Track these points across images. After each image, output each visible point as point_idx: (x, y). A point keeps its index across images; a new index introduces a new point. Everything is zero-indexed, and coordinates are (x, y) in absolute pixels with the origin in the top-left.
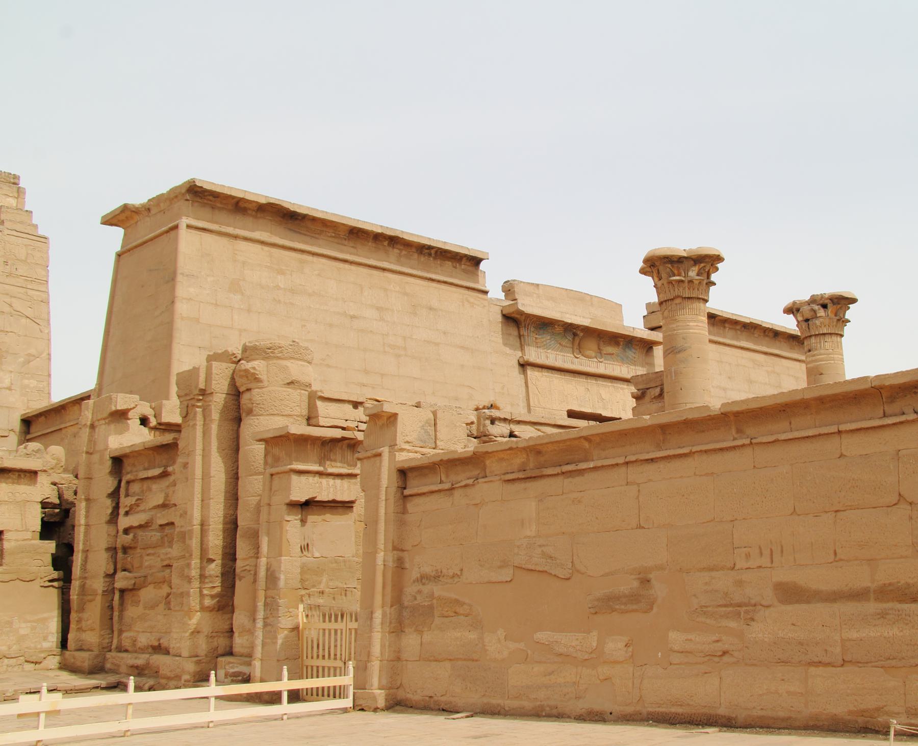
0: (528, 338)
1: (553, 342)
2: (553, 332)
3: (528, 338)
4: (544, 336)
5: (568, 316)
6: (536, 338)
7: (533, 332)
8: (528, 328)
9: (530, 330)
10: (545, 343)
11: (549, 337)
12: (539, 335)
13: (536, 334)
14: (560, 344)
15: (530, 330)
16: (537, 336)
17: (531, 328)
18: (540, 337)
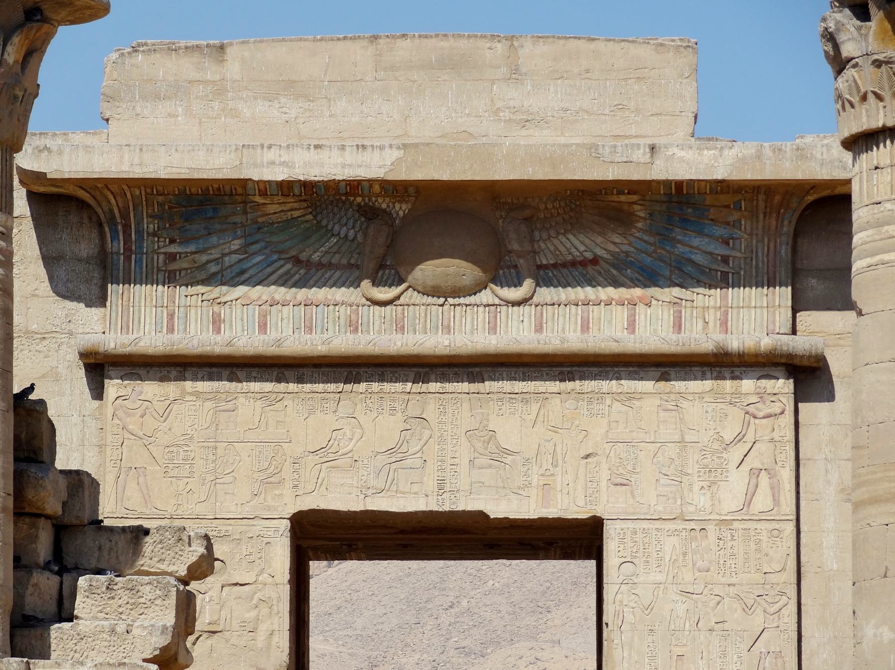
0: (128, 259)
1: (259, 258)
2: (255, 222)
3: (128, 259)
4: (214, 239)
5: (271, 155)
6: (172, 257)
7: (154, 234)
8: (127, 227)
9: (139, 232)
10: (213, 268)
11: (236, 244)
12: (185, 241)
13: (172, 241)
14: (297, 261)
15: (139, 232)
16: (174, 249)
17: (139, 223)
18: (192, 248)
